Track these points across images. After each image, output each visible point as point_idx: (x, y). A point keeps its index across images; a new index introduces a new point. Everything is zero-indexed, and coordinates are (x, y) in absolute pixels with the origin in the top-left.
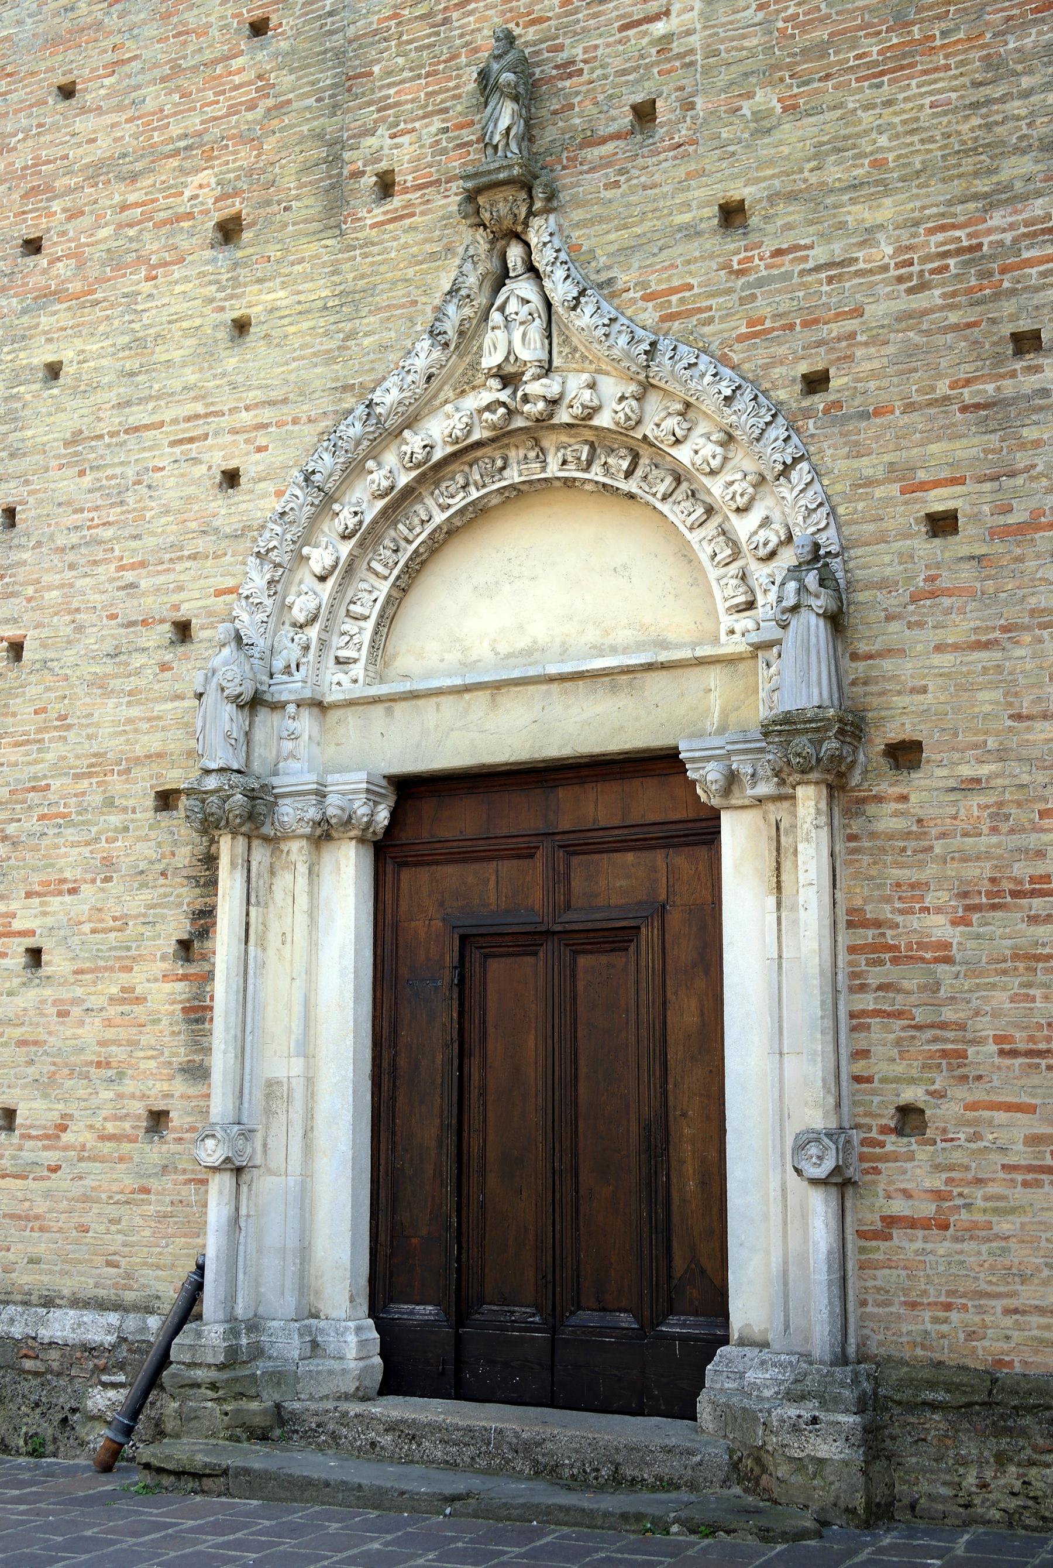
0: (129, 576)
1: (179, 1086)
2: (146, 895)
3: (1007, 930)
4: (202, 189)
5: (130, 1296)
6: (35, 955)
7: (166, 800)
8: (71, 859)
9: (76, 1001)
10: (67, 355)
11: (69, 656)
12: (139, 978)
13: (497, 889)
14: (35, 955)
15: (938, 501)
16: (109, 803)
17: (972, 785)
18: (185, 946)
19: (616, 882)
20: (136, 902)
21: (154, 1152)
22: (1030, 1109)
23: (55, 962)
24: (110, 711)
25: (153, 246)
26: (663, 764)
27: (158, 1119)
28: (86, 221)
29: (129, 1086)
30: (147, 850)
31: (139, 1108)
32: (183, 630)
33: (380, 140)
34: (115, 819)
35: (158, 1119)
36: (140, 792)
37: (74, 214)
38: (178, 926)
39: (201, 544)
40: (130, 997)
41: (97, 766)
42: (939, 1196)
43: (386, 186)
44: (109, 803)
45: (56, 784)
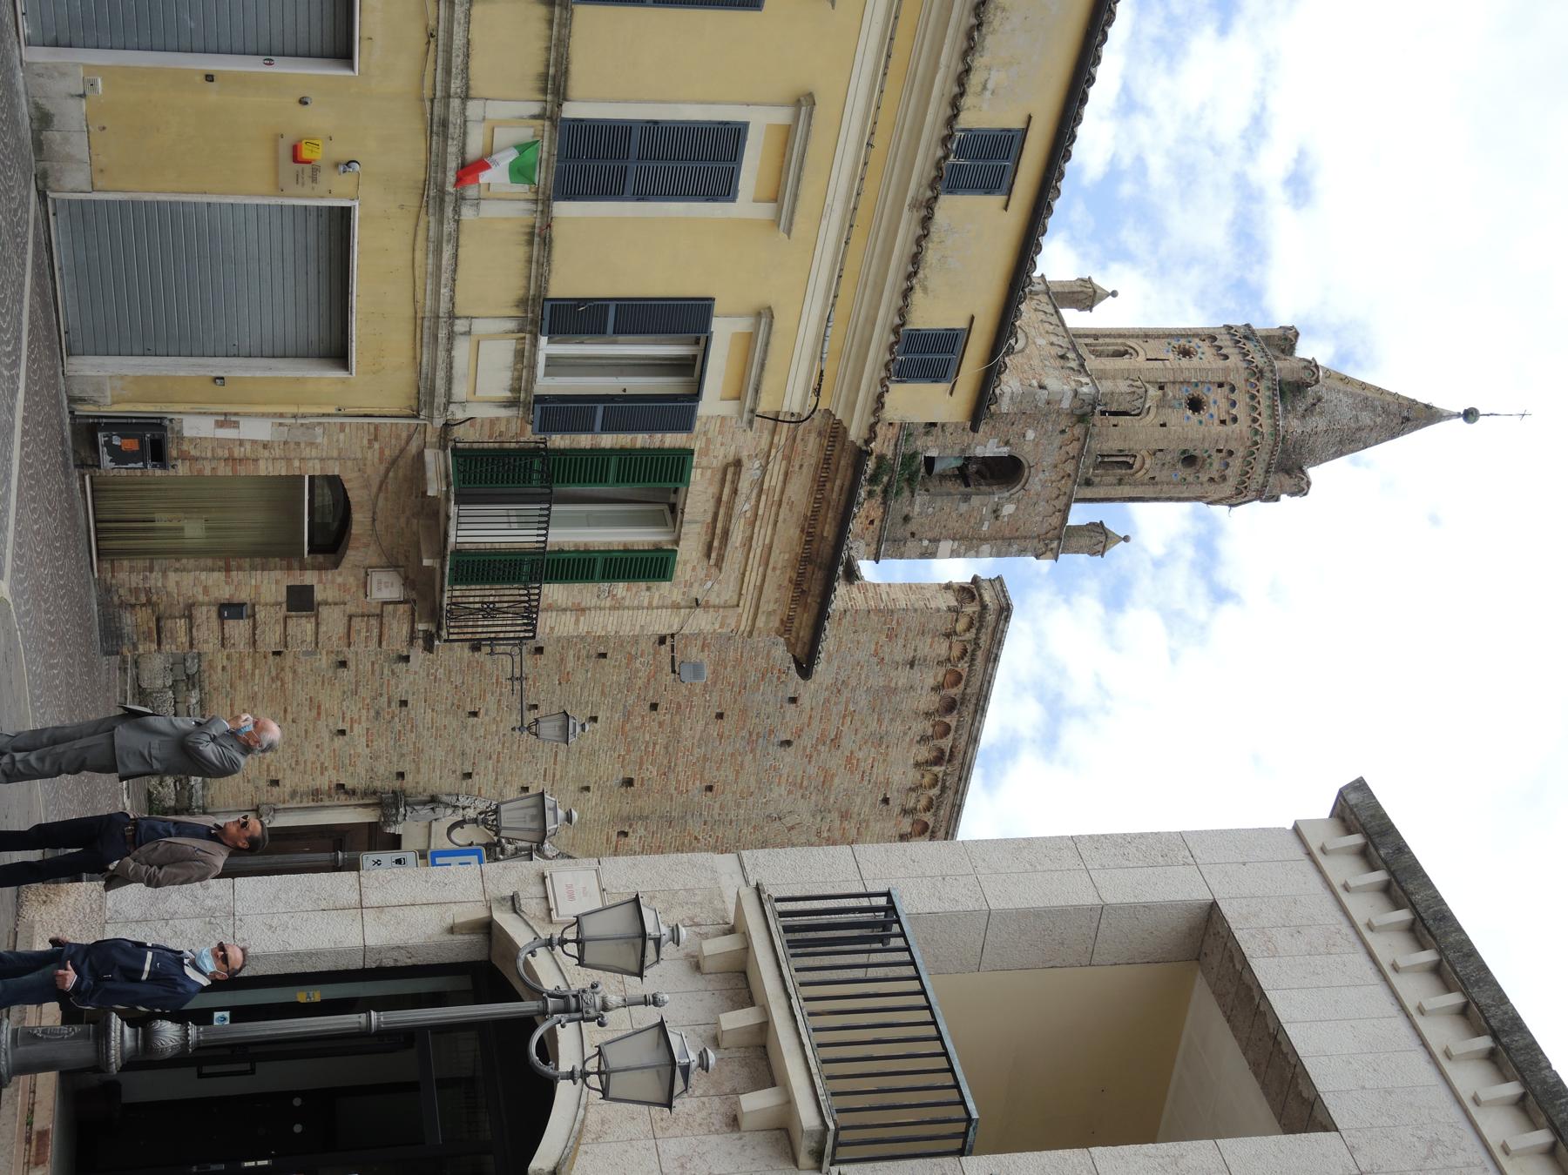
0: (495, 757)
1: (288, 790)
6: (342, 732)
7: (401, 775)
8: (380, 744)
11: (466, 736)
14: (342, 732)
16: (403, 755)
18: (341, 786)
20: (361, 770)
21: (263, 783)
23: (339, 742)
24: (440, 754)
25: (634, 756)
27: (275, 783)
28: (656, 729)
29: (289, 772)
30: (381, 770)
31: (280, 777)
32: (468, 776)
33: (642, 832)
34: (395, 759)
35: (275, 783)
36: (406, 766)
37: (661, 724)
38: (349, 785)
39: (501, 782)
40: (323, 769)
41: (418, 752)
43: (625, 834)
44: (403, 755)
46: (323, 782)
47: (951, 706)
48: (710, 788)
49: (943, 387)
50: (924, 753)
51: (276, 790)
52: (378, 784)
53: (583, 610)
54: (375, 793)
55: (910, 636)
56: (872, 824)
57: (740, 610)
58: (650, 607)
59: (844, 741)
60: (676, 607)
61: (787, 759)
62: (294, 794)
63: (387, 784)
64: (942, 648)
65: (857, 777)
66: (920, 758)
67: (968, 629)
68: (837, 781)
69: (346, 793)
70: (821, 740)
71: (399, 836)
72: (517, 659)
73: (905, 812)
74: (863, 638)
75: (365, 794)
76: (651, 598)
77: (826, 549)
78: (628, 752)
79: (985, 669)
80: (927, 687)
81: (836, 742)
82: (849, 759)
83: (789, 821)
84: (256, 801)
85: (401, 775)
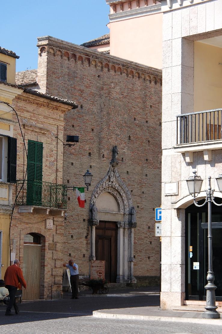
2: (83, 231)
3: (140, 242)
4: (87, 147)
5: (82, 274)
6: (72, 236)
7: (84, 220)
9: (76, 242)
10: (74, 163)
12: (82, 240)
13: (101, 232)
14: (72, 236)
15: (138, 205)
17: (138, 230)
19: (109, 233)
21: (84, 259)
22: (140, 256)
23: (74, 237)
26: (115, 223)
31: (82, 254)
33: (103, 150)
38: (85, 235)
42: (136, 263)
45: (74, 216)
46: (85, 242)
47: (74, 56)
48: (93, 130)
49: (8, 66)
50: (86, 63)
51: (86, 255)
52: (86, 227)
53: (57, 169)
54: (88, 228)
55: (54, 67)
56: (105, 81)
57: (59, 125)
58: (57, 151)
59: (82, 88)
60: (57, 143)
61: (86, 106)
62: (87, 250)
63: (85, 225)
64: (58, 58)
65: (92, 84)
66: (88, 66)
67: (53, 50)
68: (92, 91)
69: (88, 236)
70: (81, 95)
71: (100, 221)
72: (68, 188)
73: (102, 70)
74: (54, 81)
75: (88, 230)
76: (54, 150)
77: (46, 101)
78: (80, 154)
79: (65, 44)
80: (68, 62)
81: (82, 91)
82: (87, 87)
83: (103, 106)
84: (88, 261)
85: (84, 220)
